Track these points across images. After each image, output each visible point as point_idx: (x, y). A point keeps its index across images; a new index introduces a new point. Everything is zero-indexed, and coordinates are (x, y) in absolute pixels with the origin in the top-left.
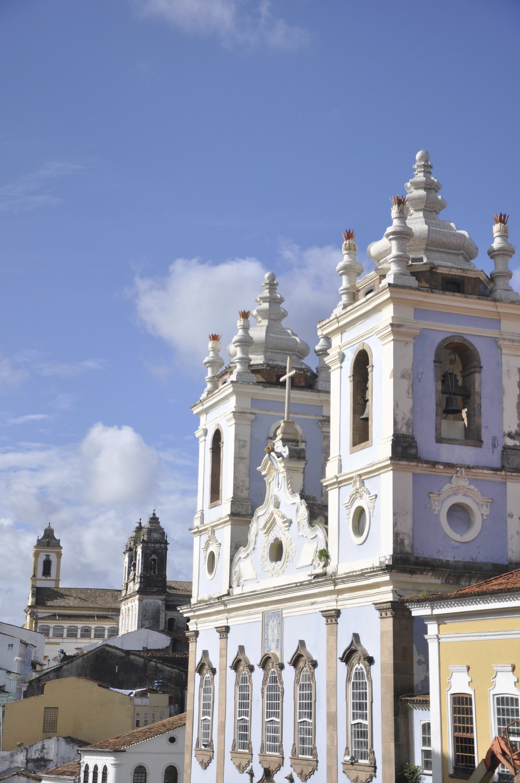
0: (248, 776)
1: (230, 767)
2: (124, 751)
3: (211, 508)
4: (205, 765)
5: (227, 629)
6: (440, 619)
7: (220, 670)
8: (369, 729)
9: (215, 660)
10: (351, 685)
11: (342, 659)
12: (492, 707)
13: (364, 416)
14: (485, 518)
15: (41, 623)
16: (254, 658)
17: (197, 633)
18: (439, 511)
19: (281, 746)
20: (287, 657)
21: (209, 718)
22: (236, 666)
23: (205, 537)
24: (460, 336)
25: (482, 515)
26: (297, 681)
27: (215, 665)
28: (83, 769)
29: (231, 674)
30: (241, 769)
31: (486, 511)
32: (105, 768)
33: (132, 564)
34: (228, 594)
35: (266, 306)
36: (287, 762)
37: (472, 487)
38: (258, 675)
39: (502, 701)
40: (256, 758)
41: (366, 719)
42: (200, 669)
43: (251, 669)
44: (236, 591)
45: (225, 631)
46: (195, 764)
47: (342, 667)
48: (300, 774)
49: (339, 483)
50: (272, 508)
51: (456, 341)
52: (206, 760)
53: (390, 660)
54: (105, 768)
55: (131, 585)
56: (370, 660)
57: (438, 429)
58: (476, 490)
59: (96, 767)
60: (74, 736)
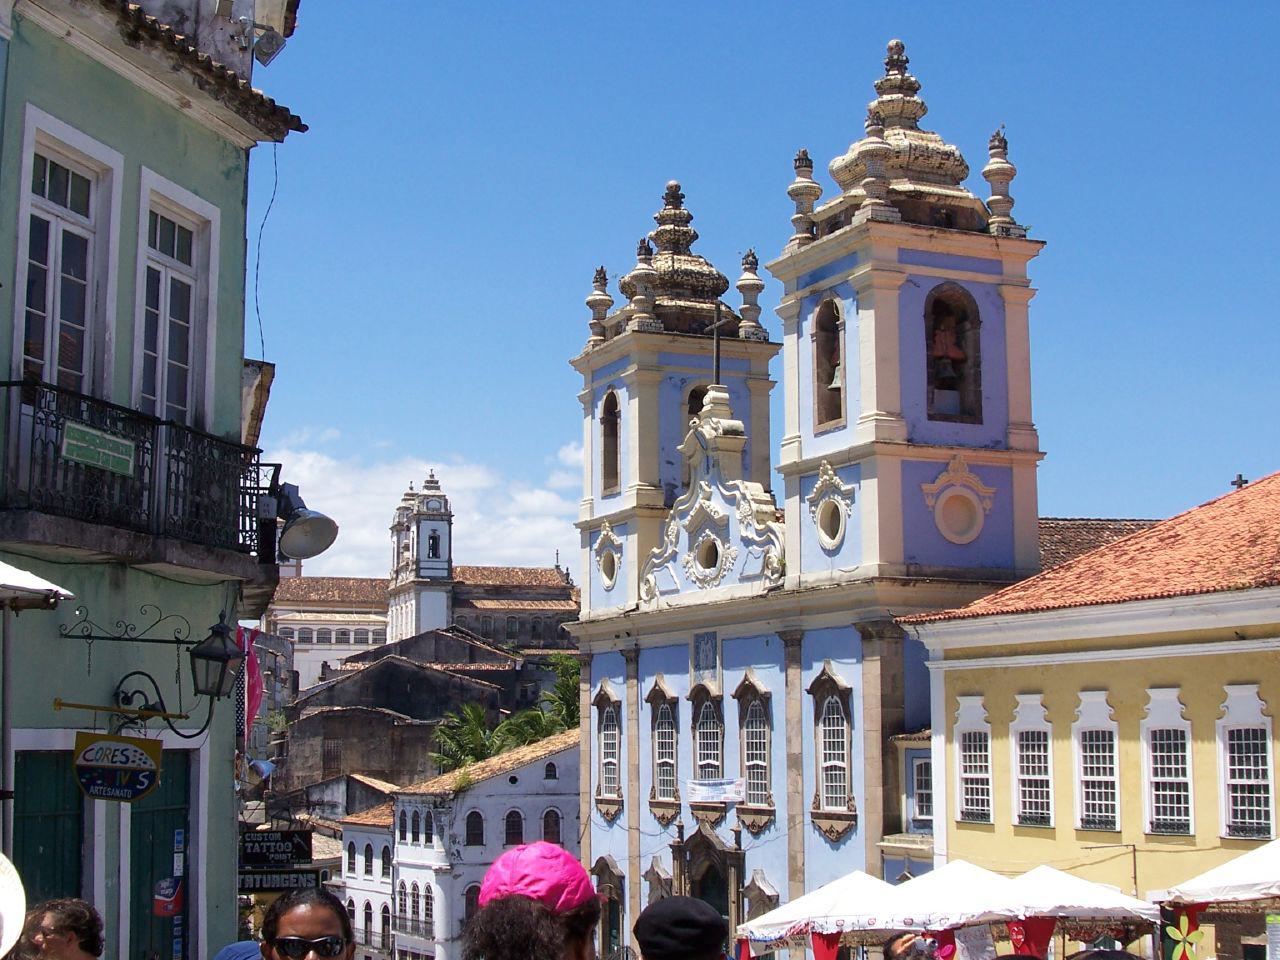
0: (673, 829)
1: (649, 823)
3: (605, 497)
4: (611, 820)
7: (629, 705)
8: (847, 772)
11: (809, 692)
13: (833, 385)
14: (987, 512)
18: (933, 507)
21: (614, 761)
25: (984, 509)
30: (665, 822)
31: (988, 504)
34: (638, 607)
41: (843, 760)
46: (596, 817)
57: (931, 401)
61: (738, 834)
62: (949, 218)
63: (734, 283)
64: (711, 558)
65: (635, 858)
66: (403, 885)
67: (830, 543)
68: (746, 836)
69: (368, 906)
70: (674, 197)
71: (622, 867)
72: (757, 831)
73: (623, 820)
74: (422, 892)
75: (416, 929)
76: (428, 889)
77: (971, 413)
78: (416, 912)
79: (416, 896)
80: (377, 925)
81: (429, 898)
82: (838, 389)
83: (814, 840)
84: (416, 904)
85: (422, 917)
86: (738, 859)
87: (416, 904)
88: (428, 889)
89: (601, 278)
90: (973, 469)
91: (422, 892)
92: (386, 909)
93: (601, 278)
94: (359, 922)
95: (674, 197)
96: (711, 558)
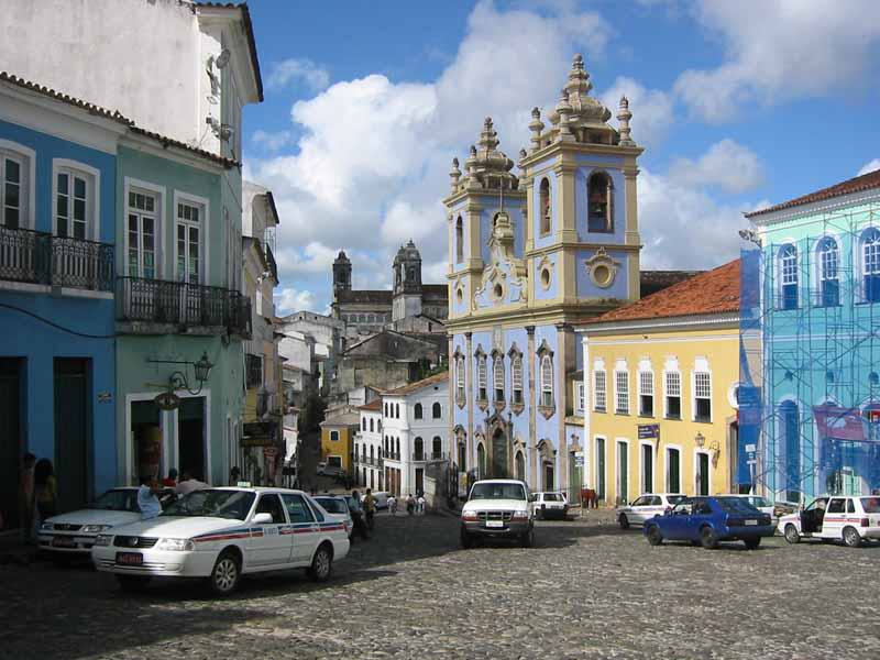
1: (476, 409)
5: (471, 334)
6: (590, 335)
9: (464, 351)
12: (615, 377)
15: (342, 314)
16: (488, 351)
17: (452, 336)
20: (506, 351)
22: (478, 354)
23: (455, 281)
29: (474, 358)
30: (482, 409)
32: (398, 405)
33: (399, 275)
35: (486, 138)
36: (508, 405)
39: (619, 375)
40: (490, 404)
42: (457, 355)
43: (486, 357)
44: (475, 314)
45: (469, 335)
48: (515, 412)
49: (533, 255)
50: (495, 267)
54: (398, 405)
55: (399, 288)
59: (392, 405)
63: (516, 164)
64: (499, 290)
65: (471, 426)
67: (546, 287)
69: (372, 447)
70: (489, 124)
71: (466, 429)
72: (518, 413)
73: (466, 407)
74: (395, 440)
75: (393, 457)
76: (398, 439)
80: (376, 456)
83: (539, 416)
85: (395, 451)
86: (511, 425)
88: (398, 439)
89: (456, 162)
93: (456, 162)
94: (361, 453)
95: (489, 124)
96: (499, 290)
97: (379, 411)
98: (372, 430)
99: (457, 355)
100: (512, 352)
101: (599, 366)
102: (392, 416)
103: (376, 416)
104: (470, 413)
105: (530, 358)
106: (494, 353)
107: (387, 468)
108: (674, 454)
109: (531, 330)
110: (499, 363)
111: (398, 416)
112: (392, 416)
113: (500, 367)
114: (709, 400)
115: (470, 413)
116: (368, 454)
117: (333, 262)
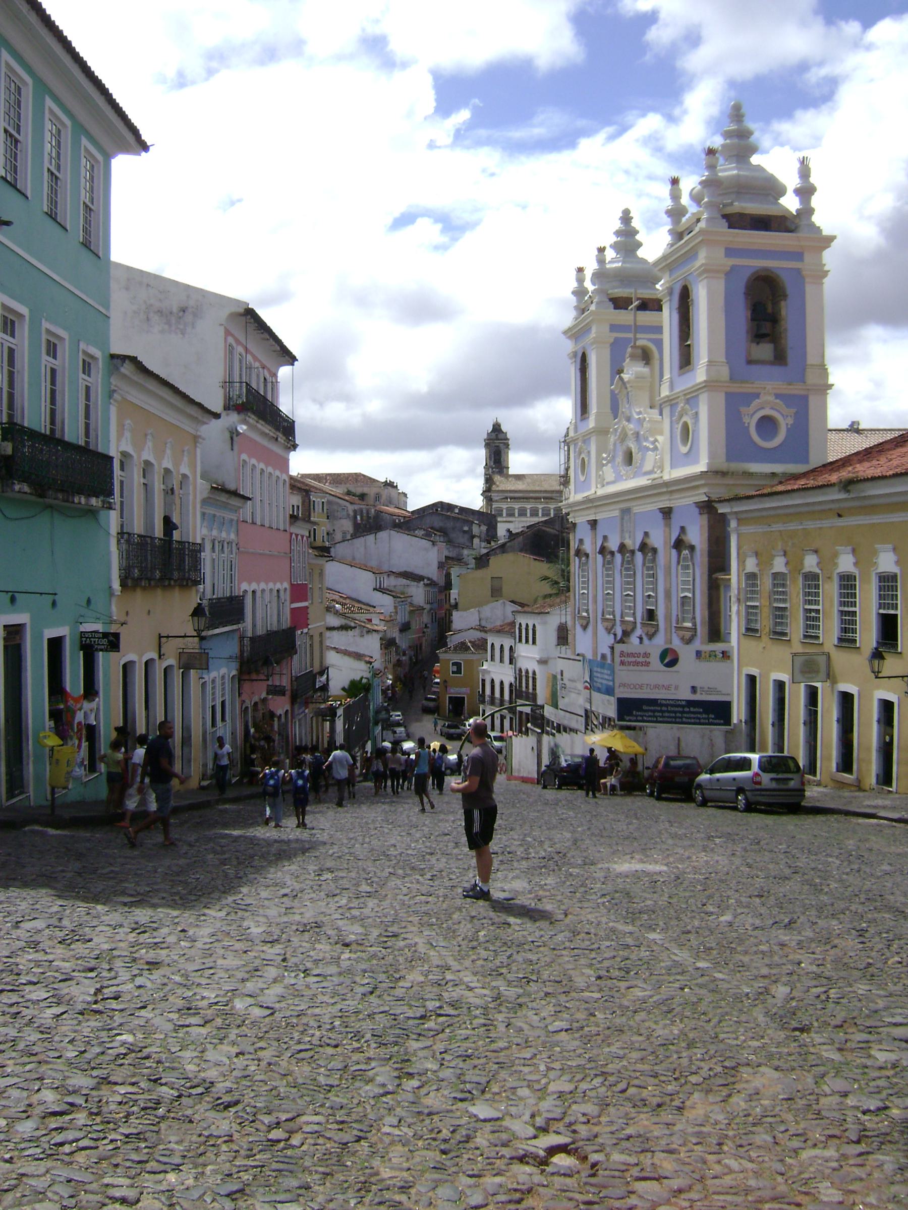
0: (612, 636)
2: (548, 613)
4: (585, 628)
9: (587, 547)
10: (680, 567)
16: (613, 545)
19: (634, 614)
22: (603, 550)
24: (766, 269)
26: (644, 564)
27: (588, 551)
28: (517, 626)
29: (599, 557)
30: (609, 630)
31: (790, 421)
32: (534, 626)
36: (639, 625)
37: (778, 401)
38: (618, 557)
47: (674, 552)
48: (647, 634)
51: (763, 274)
52: (584, 624)
53: (705, 546)
54: (534, 626)
56: (692, 548)
58: (781, 403)
60: (515, 600)
61: (641, 638)
62: (763, 223)
66: (520, 670)
67: (684, 450)
68: (645, 638)
69: (502, 683)
72: (651, 636)
73: (590, 629)
74: (531, 675)
76: (534, 673)
77: (780, 358)
78: (527, 687)
79: (527, 677)
81: (534, 679)
82: (689, 345)
84: (527, 681)
85: (531, 690)
87: (527, 681)
90: (777, 396)
91: (531, 675)
92: (511, 684)
97: (512, 634)
98: (502, 661)
99: (578, 553)
100: (643, 547)
101: (751, 565)
102: (527, 641)
103: (507, 642)
104: (595, 634)
105: (666, 556)
106: (622, 548)
107: (521, 713)
108: (846, 699)
109: (667, 513)
110: (628, 563)
111: (534, 642)
112: (527, 641)
113: (628, 564)
114: (895, 616)
115: (595, 634)
116: (497, 694)
117: (486, 437)
